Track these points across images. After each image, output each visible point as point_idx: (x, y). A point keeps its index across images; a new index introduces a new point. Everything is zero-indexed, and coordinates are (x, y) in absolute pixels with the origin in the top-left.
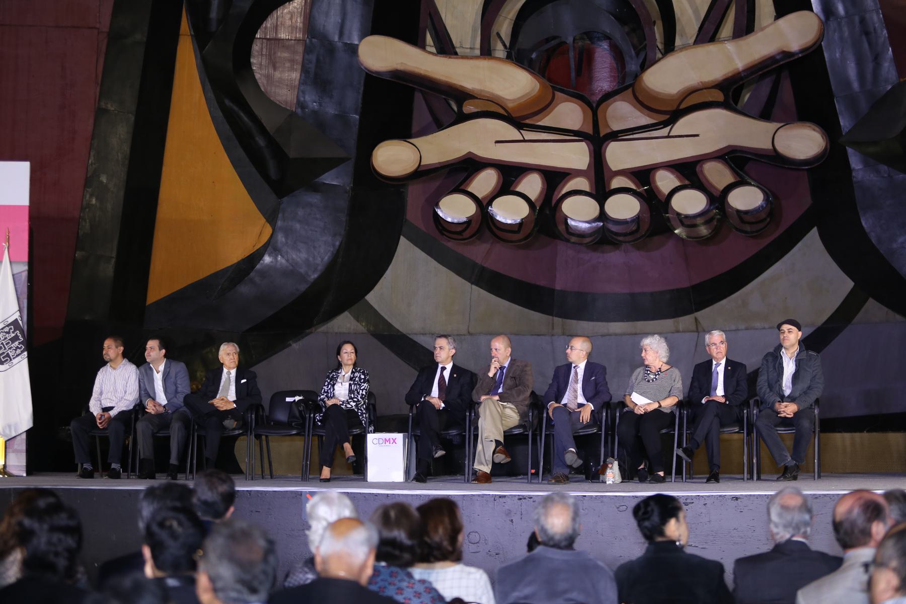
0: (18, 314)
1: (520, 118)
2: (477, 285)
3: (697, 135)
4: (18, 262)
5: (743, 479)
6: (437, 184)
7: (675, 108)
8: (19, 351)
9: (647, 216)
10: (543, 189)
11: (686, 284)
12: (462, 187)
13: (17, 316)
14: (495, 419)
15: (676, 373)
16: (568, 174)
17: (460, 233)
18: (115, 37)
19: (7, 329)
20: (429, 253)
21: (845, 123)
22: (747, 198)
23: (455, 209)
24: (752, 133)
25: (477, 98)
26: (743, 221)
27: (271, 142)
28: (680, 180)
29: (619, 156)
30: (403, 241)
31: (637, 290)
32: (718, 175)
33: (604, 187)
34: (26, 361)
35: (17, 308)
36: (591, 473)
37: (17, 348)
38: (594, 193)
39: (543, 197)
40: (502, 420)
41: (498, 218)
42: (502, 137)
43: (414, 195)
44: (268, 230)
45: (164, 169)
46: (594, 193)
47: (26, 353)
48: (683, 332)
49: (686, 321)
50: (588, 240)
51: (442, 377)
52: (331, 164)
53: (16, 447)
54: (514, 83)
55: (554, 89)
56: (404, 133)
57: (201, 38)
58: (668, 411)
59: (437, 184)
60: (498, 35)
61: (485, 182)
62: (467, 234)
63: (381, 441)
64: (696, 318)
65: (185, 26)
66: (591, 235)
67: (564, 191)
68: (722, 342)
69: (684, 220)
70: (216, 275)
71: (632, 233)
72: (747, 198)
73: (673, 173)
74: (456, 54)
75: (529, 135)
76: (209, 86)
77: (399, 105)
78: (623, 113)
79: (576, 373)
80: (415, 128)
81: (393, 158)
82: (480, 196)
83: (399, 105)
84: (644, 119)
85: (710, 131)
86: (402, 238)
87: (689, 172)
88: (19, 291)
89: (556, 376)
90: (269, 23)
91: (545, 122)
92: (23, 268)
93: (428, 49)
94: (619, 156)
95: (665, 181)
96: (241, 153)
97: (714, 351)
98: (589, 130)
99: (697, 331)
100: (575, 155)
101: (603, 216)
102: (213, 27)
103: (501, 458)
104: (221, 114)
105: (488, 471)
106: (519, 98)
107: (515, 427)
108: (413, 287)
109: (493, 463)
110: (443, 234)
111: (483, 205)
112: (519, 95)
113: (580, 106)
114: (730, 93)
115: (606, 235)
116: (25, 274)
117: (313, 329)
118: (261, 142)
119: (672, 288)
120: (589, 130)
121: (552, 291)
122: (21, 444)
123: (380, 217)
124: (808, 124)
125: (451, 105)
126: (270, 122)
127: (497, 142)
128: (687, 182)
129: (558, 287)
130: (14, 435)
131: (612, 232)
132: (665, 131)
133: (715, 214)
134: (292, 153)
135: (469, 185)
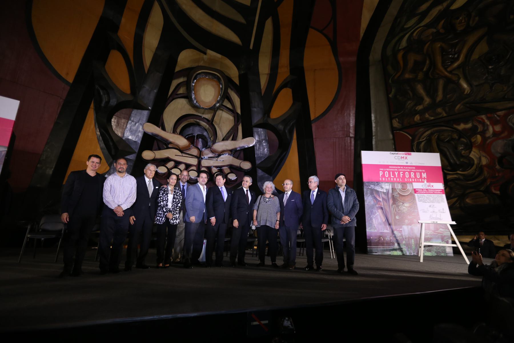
1: (182, 150)
21: (258, 162)
24: (237, 162)
29: (205, 163)
32: (226, 170)
44: (108, 168)
54: (182, 142)
56: (151, 149)
57: (97, 110)
61: (171, 164)
75: (184, 155)
76: (97, 126)
78: (207, 154)
85: (226, 159)
95: (214, 170)
96: (103, 145)
98: (198, 156)
100: (194, 161)
114: (234, 152)
118: (111, 144)
120: (198, 156)
125: (165, 144)
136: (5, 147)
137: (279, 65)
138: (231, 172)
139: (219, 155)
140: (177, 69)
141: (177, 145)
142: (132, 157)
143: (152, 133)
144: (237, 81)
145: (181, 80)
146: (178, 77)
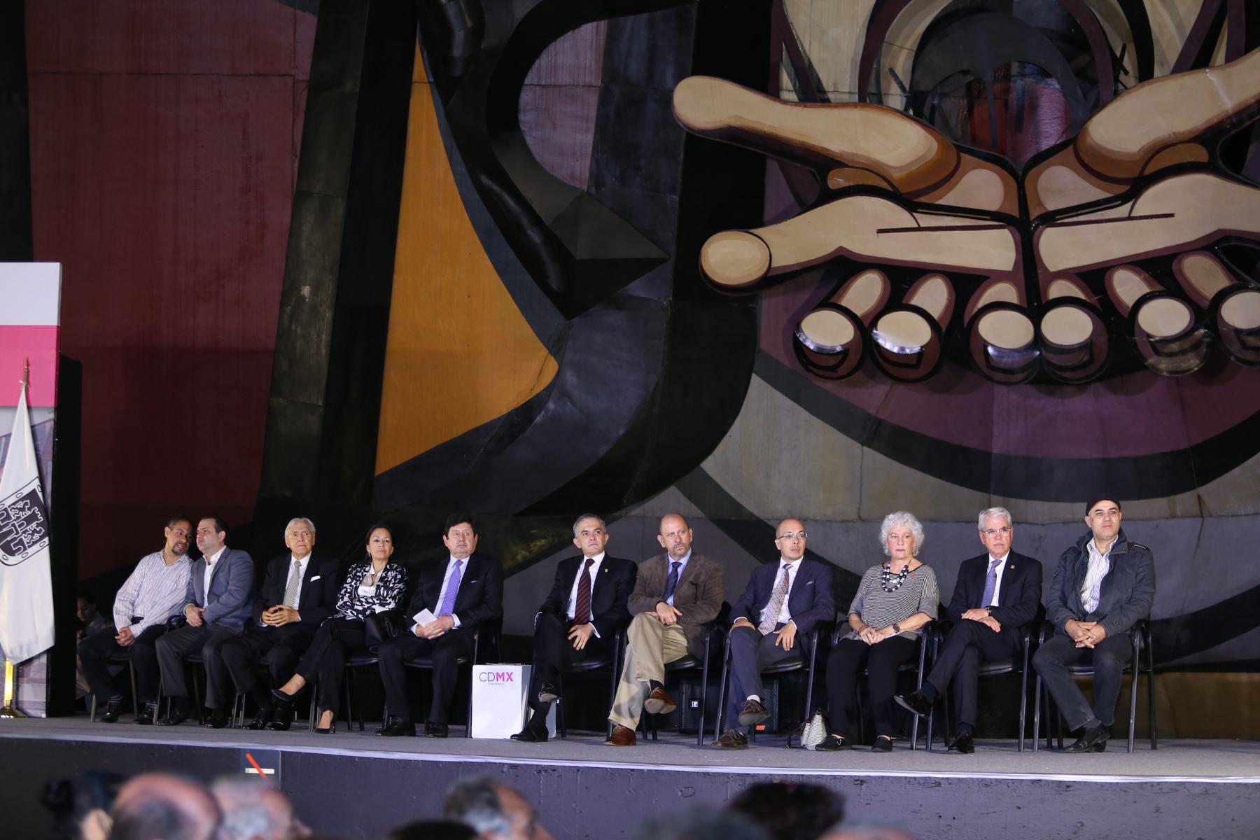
0: (37, 482)
2: (869, 446)
3: (1172, 215)
4: (39, 408)
5: (1032, 747)
6: (805, 296)
7: (1137, 175)
8: (37, 536)
9: (1103, 339)
10: (949, 301)
11: (1184, 445)
13: (36, 485)
14: (651, 646)
15: (929, 575)
16: (986, 278)
17: (833, 368)
18: (317, 87)
19: (20, 505)
20: (796, 399)
23: (826, 331)
25: (847, 166)
27: (550, 237)
28: (1149, 285)
30: (755, 380)
31: (1113, 453)
32: (1205, 275)
33: (1039, 300)
34: (47, 550)
35: (36, 474)
36: (785, 730)
37: (35, 531)
38: (1025, 305)
40: (662, 648)
41: (881, 341)
42: (882, 220)
43: (770, 310)
44: (552, 366)
45: (396, 277)
46: (1025, 305)
47: (46, 539)
48: (1183, 517)
49: (1185, 500)
50: (1020, 377)
51: (586, 574)
52: (641, 267)
53: (32, 675)
54: (898, 142)
55: (960, 149)
57: (444, 85)
58: (913, 638)
59: (805, 296)
60: (892, 71)
61: (865, 292)
62: (844, 369)
63: (491, 677)
64: (1199, 497)
65: (420, 69)
66: (1022, 370)
67: (981, 304)
68: (1004, 529)
69: (1158, 345)
70: (476, 432)
73: (1139, 274)
74: (828, 101)
77: (744, 179)
78: (1060, 184)
79: (787, 576)
80: (769, 212)
81: (731, 257)
82: (859, 313)
83: (744, 179)
84: (1095, 193)
86: (754, 376)
87: (1161, 271)
88: (41, 449)
89: (754, 582)
90: (544, 60)
91: (949, 199)
92: (46, 417)
93: (786, 95)
94: (1061, 249)
95: (1127, 287)
97: (990, 541)
98: (1014, 211)
99: (1202, 516)
100: (992, 250)
101: (1039, 339)
102: (458, 72)
103: (655, 706)
104: (478, 197)
105: (633, 727)
107: (684, 659)
108: (775, 449)
109: (645, 714)
110: (809, 371)
111: (865, 326)
112: (908, 161)
113: (999, 174)
115: (1044, 368)
116: (50, 426)
117: (623, 512)
118: (535, 236)
119: (1164, 450)
120: (1014, 211)
121: (987, 456)
122: (39, 671)
123: (720, 345)
125: (816, 178)
126: (546, 206)
127: (880, 231)
128: (1159, 288)
129: (996, 449)
130: (26, 657)
131: (1054, 365)
132: (1123, 210)
133: (1204, 336)
134: (580, 253)
135: (841, 296)
136: (48, 409)
141: (872, 168)
142: (649, 290)
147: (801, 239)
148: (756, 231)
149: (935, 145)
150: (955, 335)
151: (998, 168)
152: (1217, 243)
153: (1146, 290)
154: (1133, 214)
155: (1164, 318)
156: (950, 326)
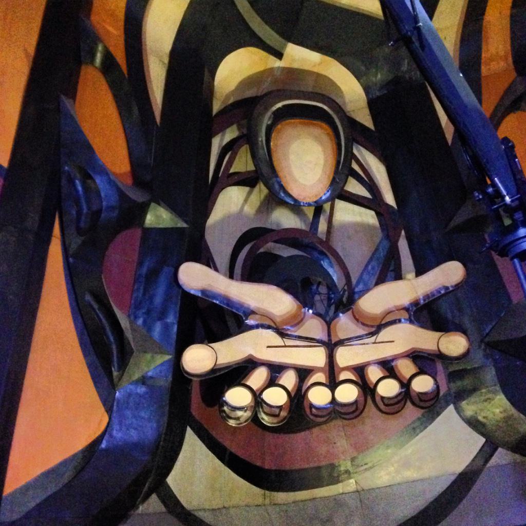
3: (393, 341)
12: (243, 382)
22: (423, 384)
23: (237, 397)
25: (257, 314)
26: (421, 400)
32: (406, 368)
33: (335, 381)
39: (296, 388)
61: (258, 378)
71: (354, 412)
72: (423, 384)
75: (289, 342)
81: (199, 359)
82: (255, 388)
87: (388, 367)
91: (301, 332)
94: (346, 357)
95: (374, 373)
98: (325, 338)
100: (316, 357)
106: (284, 315)
120: (325, 339)
124: (460, 333)
132: (373, 339)
135: (246, 381)
137: (483, 55)
138: (421, 372)
139: (379, 328)
140: (216, 107)
143: (203, 292)
144: (365, 118)
145: (230, 134)
146: (222, 130)
147: (230, 351)
148: (211, 345)
149: (296, 306)
150: (298, 398)
151: (320, 319)
152: (411, 354)
153: (382, 375)
154: (376, 341)
155: (388, 388)
156: (296, 394)
